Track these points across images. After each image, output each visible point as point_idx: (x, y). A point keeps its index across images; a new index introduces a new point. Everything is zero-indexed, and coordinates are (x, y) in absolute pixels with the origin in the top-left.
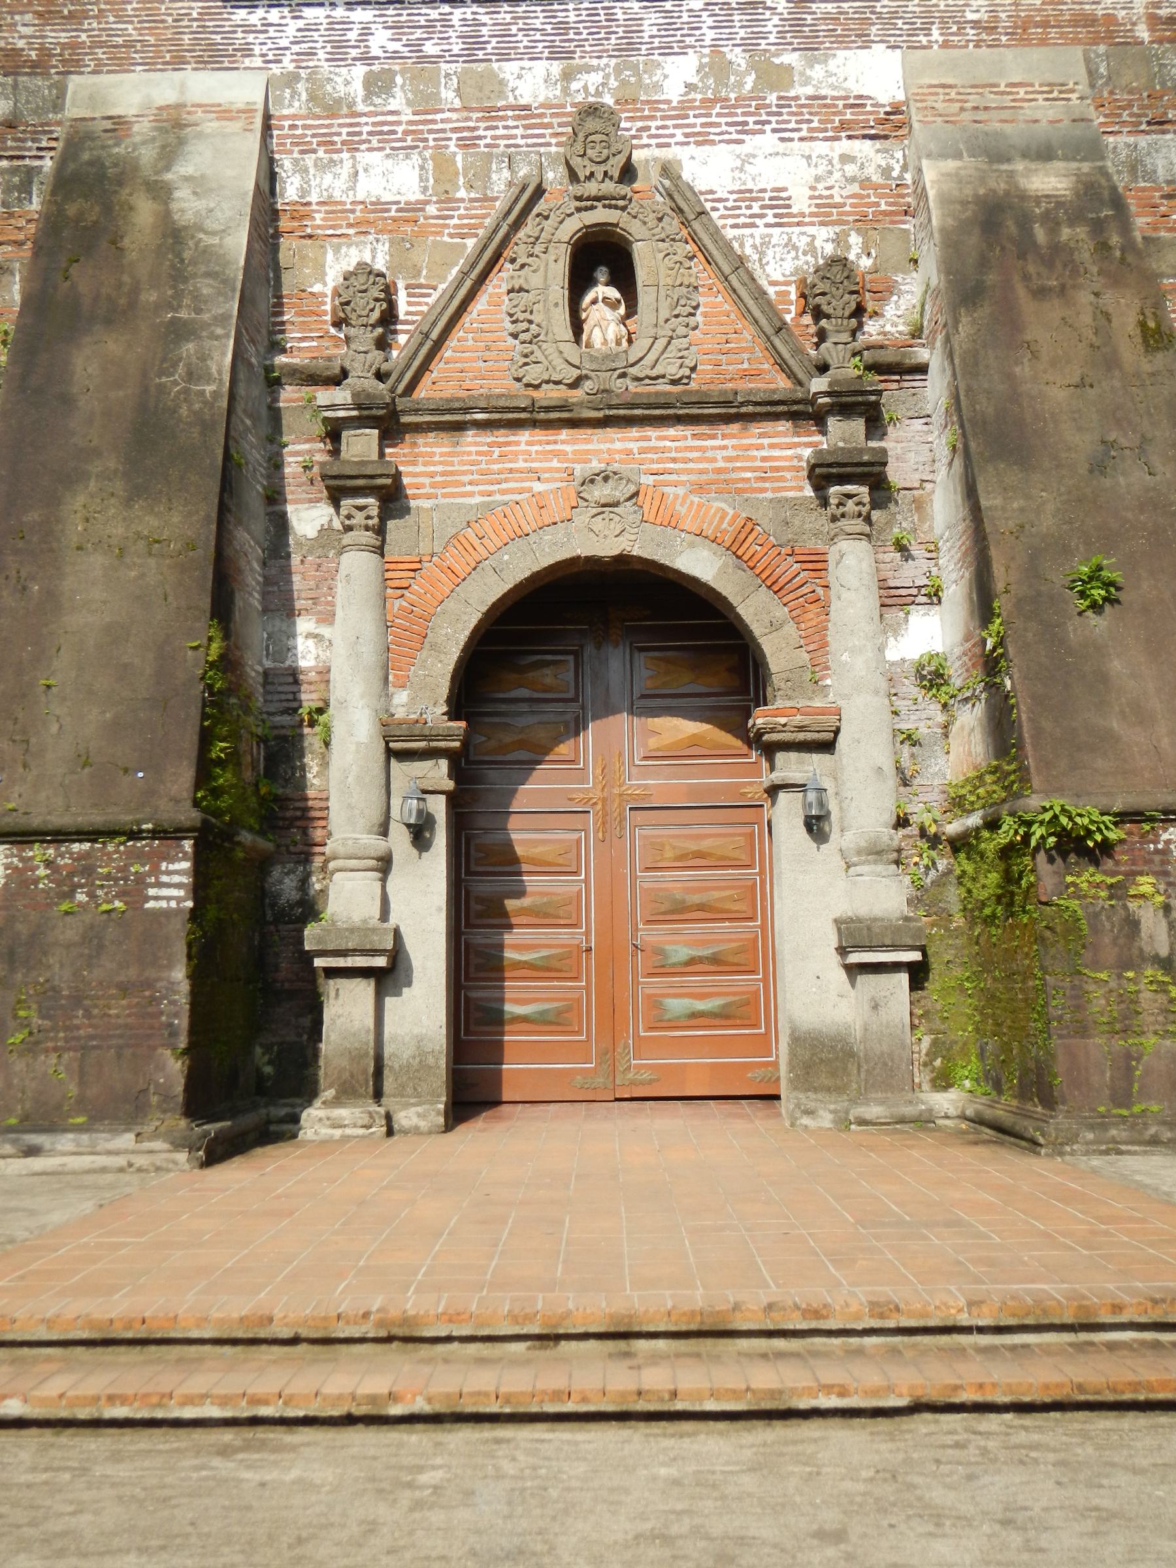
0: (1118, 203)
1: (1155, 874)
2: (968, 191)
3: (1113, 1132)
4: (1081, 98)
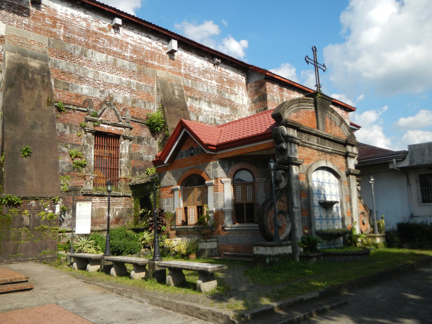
0: (49, 73)
1: (29, 210)
2: (15, 61)
3: (11, 260)
4: (46, 48)
